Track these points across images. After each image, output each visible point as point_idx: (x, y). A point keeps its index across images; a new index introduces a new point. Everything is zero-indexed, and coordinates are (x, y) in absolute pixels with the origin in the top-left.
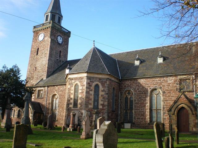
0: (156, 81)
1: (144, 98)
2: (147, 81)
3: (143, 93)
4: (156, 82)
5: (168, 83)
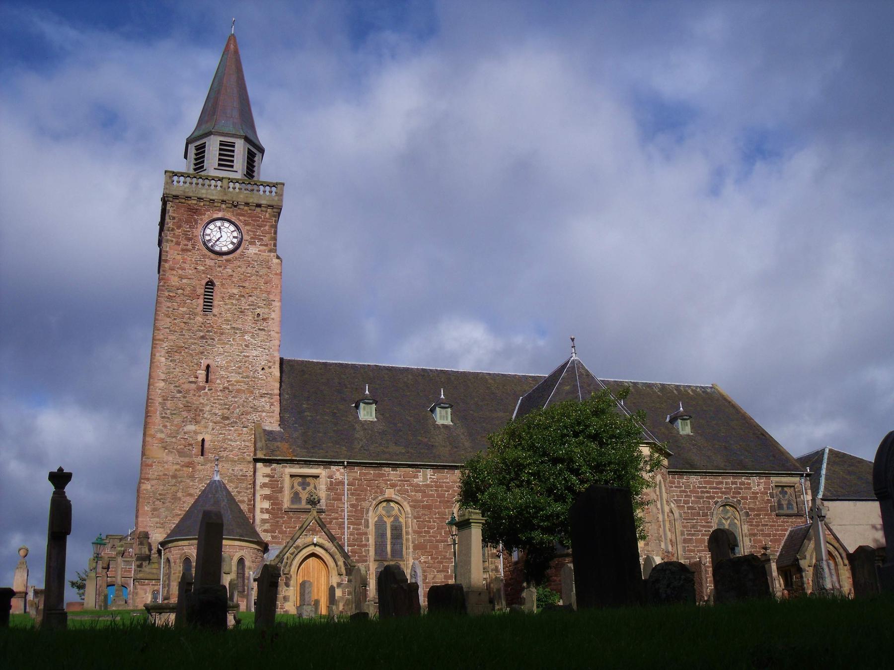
0: (727, 483)
1: (704, 526)
2: (706, 482)
3: (699, 514)
4: (728, 488)
5: (753, 493)
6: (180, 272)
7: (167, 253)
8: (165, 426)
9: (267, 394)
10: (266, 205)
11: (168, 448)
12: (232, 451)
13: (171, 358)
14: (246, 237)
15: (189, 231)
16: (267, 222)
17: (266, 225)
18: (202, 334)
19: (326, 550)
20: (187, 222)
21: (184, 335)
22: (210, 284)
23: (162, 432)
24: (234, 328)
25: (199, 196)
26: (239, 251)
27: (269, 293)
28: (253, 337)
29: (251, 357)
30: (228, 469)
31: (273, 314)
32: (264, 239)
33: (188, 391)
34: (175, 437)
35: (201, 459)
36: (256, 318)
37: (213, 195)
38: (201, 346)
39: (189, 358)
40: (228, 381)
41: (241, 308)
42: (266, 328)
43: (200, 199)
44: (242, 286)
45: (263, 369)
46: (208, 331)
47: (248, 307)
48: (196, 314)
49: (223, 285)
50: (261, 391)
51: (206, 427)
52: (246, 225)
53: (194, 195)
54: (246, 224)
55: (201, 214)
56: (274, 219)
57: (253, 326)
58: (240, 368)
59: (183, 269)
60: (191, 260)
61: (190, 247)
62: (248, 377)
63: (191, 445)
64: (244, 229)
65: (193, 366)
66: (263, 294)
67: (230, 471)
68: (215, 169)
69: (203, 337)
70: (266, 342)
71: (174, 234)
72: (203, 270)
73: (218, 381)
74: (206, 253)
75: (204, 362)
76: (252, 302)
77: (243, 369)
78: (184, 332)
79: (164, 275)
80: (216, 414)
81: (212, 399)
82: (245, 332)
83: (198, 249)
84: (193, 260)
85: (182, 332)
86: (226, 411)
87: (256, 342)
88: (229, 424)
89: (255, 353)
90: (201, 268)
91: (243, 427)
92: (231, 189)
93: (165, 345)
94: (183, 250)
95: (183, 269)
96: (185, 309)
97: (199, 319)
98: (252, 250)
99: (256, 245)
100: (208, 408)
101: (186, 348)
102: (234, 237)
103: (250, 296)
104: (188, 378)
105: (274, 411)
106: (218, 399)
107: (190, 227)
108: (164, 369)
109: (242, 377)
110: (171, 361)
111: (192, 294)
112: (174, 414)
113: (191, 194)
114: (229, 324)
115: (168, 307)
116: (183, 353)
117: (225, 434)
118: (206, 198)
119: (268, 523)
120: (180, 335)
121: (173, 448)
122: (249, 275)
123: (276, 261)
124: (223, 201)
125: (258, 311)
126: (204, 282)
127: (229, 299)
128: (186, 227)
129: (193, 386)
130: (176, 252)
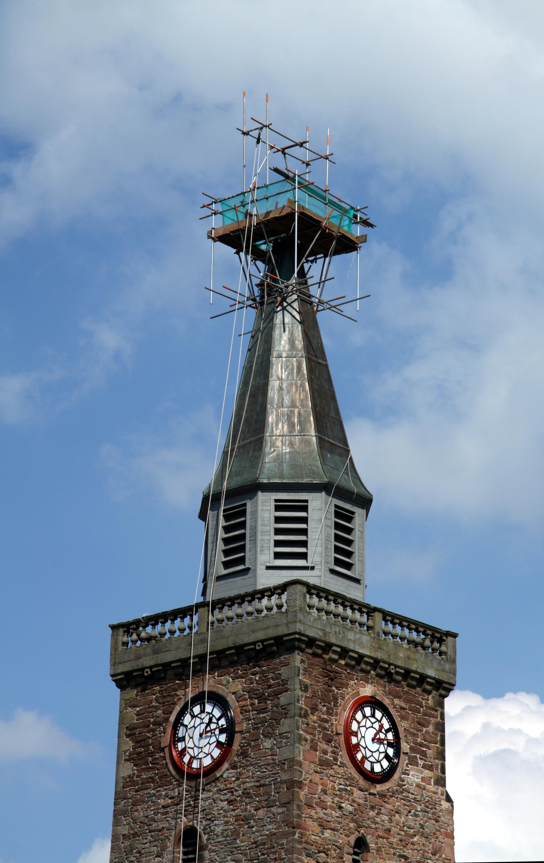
7: (300, 766)
14: (405, 747)
20: (325, 699)
25: (344, 644)
37: (363, 647)
43: (344, 652)
52: (403, 718)
53: (338, 643)
61: (329, 756)
64: (402, 725)
71: (308, 724)
79: (299, 816)
83: (342, 765)
113: (333, 640)
123: (445, 805)
124: (376, 663)
126: (352, 839)
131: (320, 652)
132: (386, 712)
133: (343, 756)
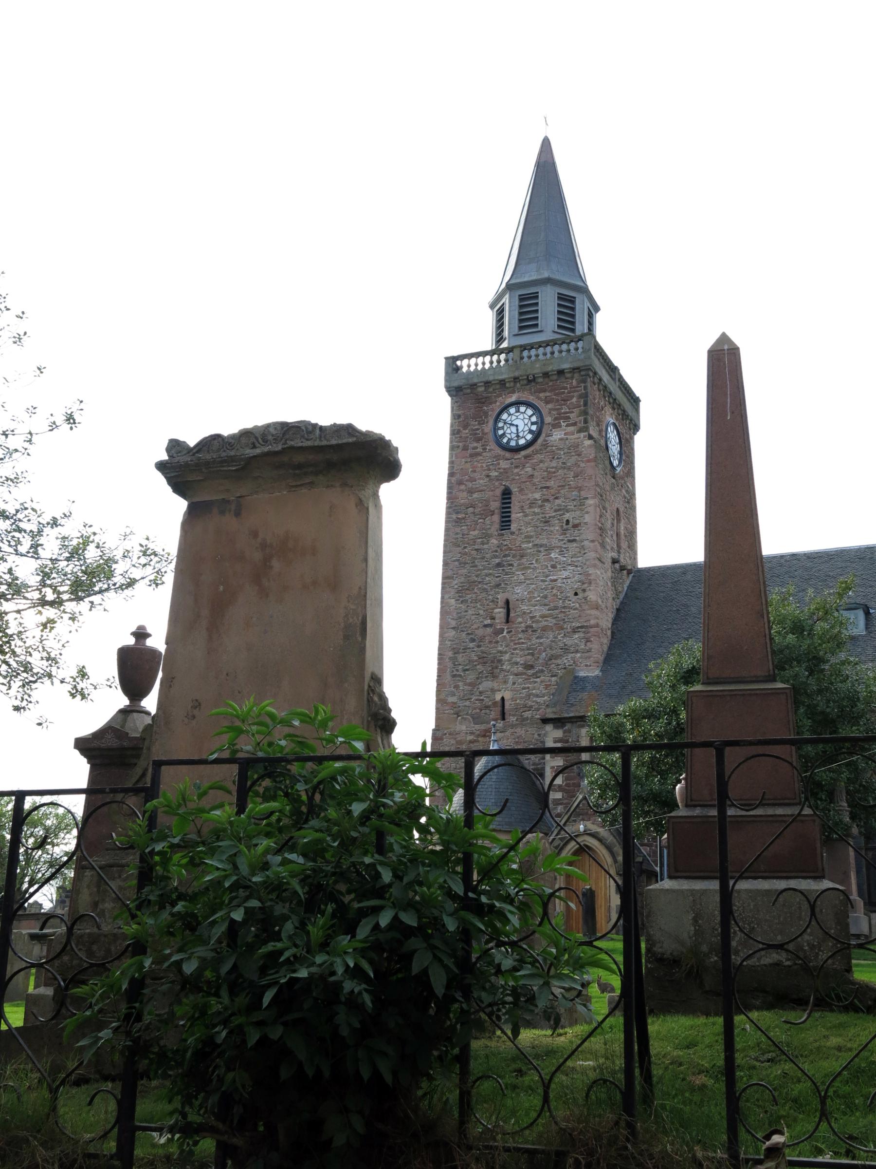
6: (470, 485)
8: (457, 687)
9: (582, 627)
10: (570, 368)
11: (461, 714)
12: (538, 710)
13: (461, 599)
14: (548, 419)
15: (478, 429)
16: (575, 391)
17: (573, 397)
18: (497, 561)
19: (600, 840)
20: (474, 418)
21: (476, 566)
22: (507, 494)
23: (455, 695)
24: (537, 545)
26: (540, 441)
27: (579, 489)
28: (561, 553)
29: (560, 580)
30: (533, 734)
31: (586, 516)
32: (572, 415)
33: (482, 639)
34: (468, 699)
35: (500, 724)
36: (565, 527)
38: (497, 577)
39: (484, 595)
40: (532, 618)
41: (545, 517)
42: (577, 538)
43: (487, 384)
44: (545, 487)
45: (576, 594)
46: (505, 556)
47: (554, 514)
48: (491, 536)
49: (521, 490)
50: (574, 624)
51: (505, 682)
52: (547, 402)
53: (480, 380)
54: (547, 401)
55: (491, 403)
56: (583, 385)
57: (561, 537)
58: (545, 597)
59: (472, 480)
60: (482, 467)
61: (480, 450)
62: (556, 608)
63: (487, 707)
64: (545, 409)
65: (488, 605)
66: (573, 491)
67: (536, 736)
68: (515, 335)
69: (499, 565)
70: (578, 557)
72: (496, 476)
73: (520, 620)
74: (499, 451)
75: (501, 597)
76: (558, 505)
77: (550, 598)
78: (476, 561)
80: (517, 663)
81: (512, 644)
82: (549, 549)
84: (484, 465)
85: (474, 562)
86: (530, 657)
87: (565, 559)
88: (533, 674)
89: (565, 574)
90: (494, 474)
91: (552, 676)
92: (526, 359)
93: (456, 582)
94: (471, 456)
95: (472, 480)
96: (476, 532)
97: (494, 541)
98: (557, 435)
99: (560, 427)
100: (507, 657)
101: (480, 582)
102: (533, 424)
103: (557, 498)
104: (482, 622)
105: (591, 649)
106: (519, 643)
107: (479, 424)
108: (454, 614)
109: (549, 610)
110: (462, 602)
111: (484, 510)
112: (467, 670)
114: (530, 542)
115: (457, 534)
116: (476, 590)
117: (528, 688)
118: (494, 380)
119: (561, 804)
120: (471, 567)
121: (467, 714)
122: (554, 470)
123: (588, 442)
124: (516, 379)
125: (567, 516)
126: (498, 492)
127: (530, 507)
128: (474, 424)
129: (489, 630)
130: (463, 460)
131: (469, 391)
132: (528, 405)
133: (492, 445)
